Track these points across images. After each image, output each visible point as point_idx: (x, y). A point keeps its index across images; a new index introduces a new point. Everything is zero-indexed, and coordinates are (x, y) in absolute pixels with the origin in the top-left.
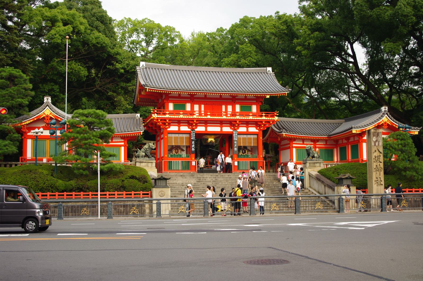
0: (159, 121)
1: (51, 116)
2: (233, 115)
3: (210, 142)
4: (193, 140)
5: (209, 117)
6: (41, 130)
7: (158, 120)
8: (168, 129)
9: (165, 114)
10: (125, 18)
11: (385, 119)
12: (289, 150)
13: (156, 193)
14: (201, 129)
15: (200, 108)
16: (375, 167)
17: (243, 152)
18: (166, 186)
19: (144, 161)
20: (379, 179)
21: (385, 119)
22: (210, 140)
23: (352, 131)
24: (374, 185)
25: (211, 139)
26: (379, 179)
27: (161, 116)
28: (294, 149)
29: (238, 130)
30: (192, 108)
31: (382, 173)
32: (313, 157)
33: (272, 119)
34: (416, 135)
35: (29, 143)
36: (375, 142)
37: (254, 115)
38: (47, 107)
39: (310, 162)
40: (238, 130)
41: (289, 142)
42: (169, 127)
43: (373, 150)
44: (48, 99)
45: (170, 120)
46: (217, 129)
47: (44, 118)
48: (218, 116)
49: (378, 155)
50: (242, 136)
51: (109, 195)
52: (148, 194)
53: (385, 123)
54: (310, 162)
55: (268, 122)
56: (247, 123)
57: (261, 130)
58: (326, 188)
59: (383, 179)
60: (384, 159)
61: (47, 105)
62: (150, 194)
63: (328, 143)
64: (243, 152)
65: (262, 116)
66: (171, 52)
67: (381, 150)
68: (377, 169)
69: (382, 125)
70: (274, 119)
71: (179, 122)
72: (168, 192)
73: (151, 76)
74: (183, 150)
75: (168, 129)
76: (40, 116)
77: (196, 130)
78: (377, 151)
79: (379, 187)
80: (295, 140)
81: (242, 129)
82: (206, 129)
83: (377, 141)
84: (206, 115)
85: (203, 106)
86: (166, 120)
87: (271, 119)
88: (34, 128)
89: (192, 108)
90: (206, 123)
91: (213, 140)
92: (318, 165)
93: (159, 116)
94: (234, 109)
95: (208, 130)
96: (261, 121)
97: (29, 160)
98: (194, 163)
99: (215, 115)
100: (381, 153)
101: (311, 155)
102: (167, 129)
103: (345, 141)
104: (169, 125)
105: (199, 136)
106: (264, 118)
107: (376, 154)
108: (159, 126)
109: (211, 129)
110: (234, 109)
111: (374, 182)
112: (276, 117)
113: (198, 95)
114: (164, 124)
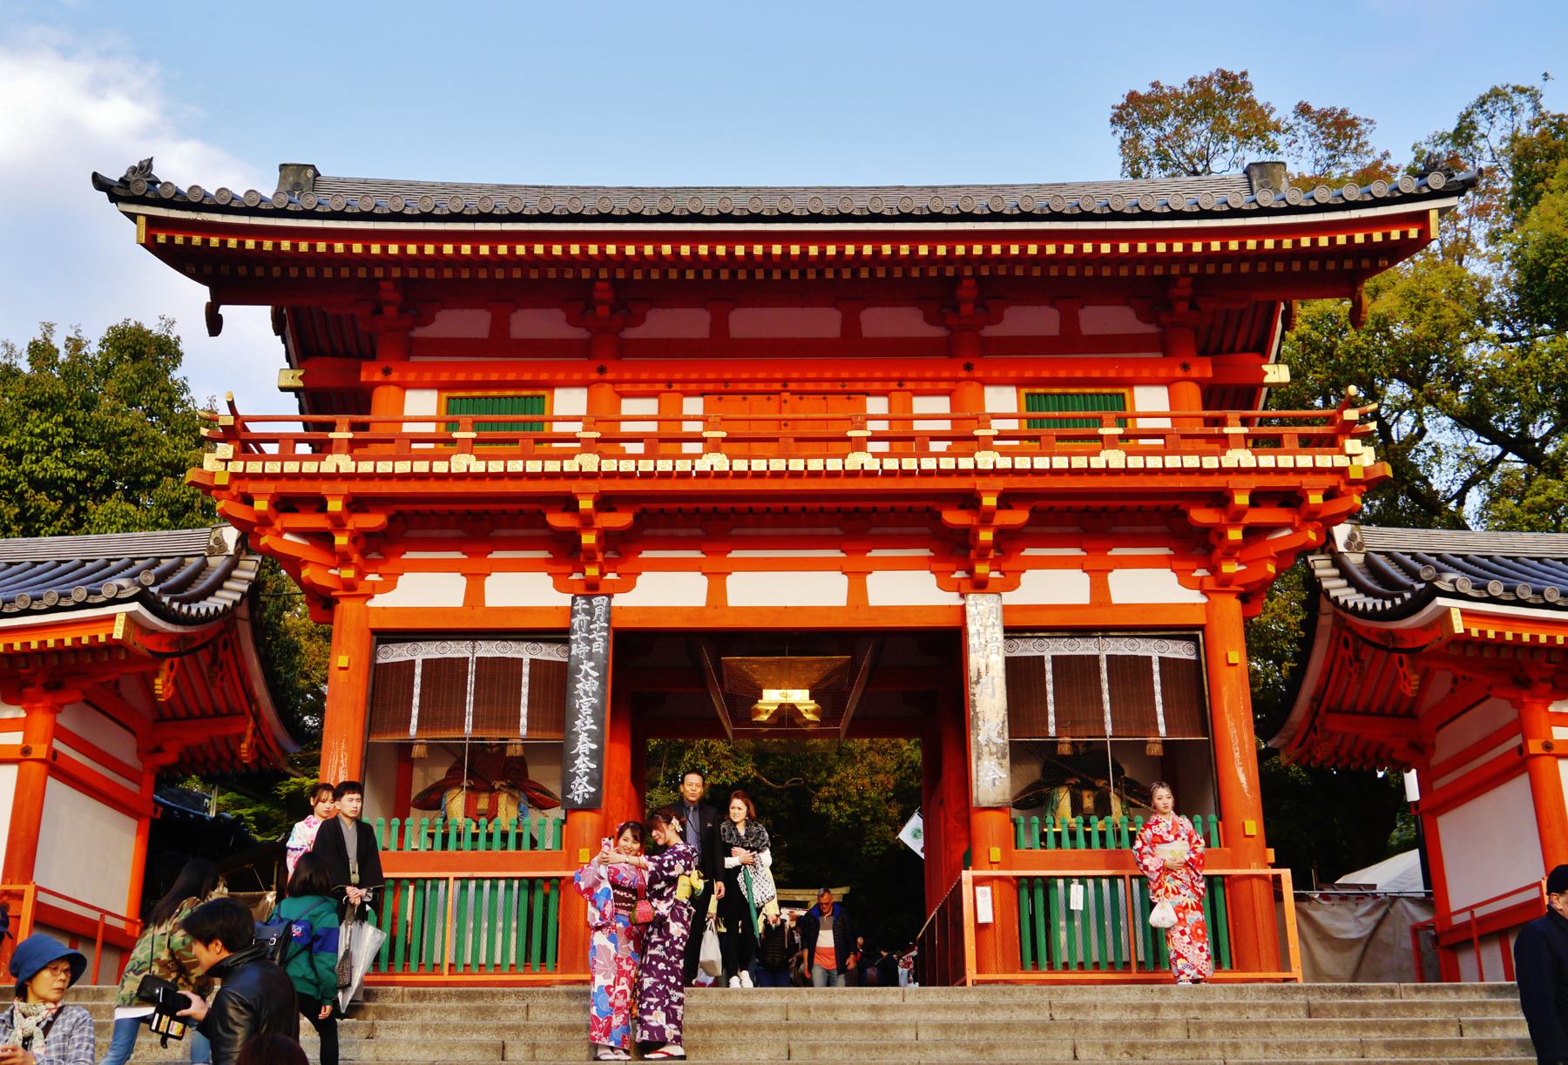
0: (261, 505)
7: (248, 500)
8: (379, 601)
14: (667, 590)
17: (1088, 802)
22: (772, 698)
33: (1324, 461)
55: (1283, 496)
57: (1224, 583)
64: (1088, 802)
65: (1224, 442)
70: (1341, 461)
82: (717, 592)
91: (800, 698)
106: (1239, 457)
112: (1352, 445)
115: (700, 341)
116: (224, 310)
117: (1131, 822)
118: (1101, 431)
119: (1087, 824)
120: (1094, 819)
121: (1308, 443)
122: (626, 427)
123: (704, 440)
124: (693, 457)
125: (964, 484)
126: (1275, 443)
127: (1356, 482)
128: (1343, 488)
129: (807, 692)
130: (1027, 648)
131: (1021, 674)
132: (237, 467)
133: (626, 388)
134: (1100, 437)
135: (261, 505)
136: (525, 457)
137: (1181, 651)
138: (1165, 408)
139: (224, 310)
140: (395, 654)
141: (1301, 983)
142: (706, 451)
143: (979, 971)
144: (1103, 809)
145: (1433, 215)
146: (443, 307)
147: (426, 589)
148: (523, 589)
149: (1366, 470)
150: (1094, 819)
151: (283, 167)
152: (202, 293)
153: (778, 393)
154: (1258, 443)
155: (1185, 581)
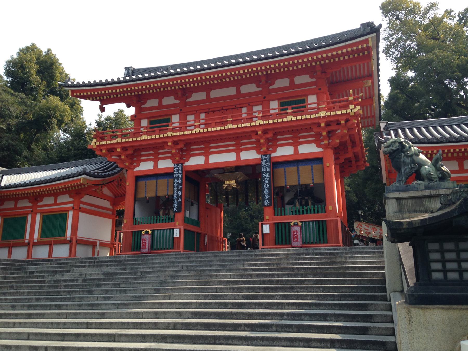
7: (101, 150)
8: (136, 169)
14: (196, 161)
17: (303, 203)
27: (105, 143)
29: (273, 155)
33: (344, 112)
39: (397, 195)
46: (228, 158)
48: (217, 124)
54: (397, 195)
64: (303, 203)
70: (348, 111)
87: (339, 112)
93: (101, 143)
101: (405, 169)
109: (215, 159)
115: (234, 95)
116: (105, 106)
117: (314, 207)
118: (287, 111)
119: (303, 208)
120: (305, 207)
121: (341, 108)
122: (188, 123)
123: (195, 126)
124: (191, 130)
125: (253, 129)
126: (334, 109)
127: (353, 116)
128: (350, 118)
129: (234, 181)
132: (98, 143)
133: (185, 114)
134: (287, 113)
135: (104, 151)
136: (129, 138)
138: (316, 101)
139: (105, 106)
141: (182, 253)
142: (195, 128)
143: (263, 245)
144: (307, 204)
145: (370, 40)
146: (148, 99)
149: (355, 112)
150: (305, 207)
151: (126, 68)
152: (98, 103)
153: (221, 110)
155: (318, 146)
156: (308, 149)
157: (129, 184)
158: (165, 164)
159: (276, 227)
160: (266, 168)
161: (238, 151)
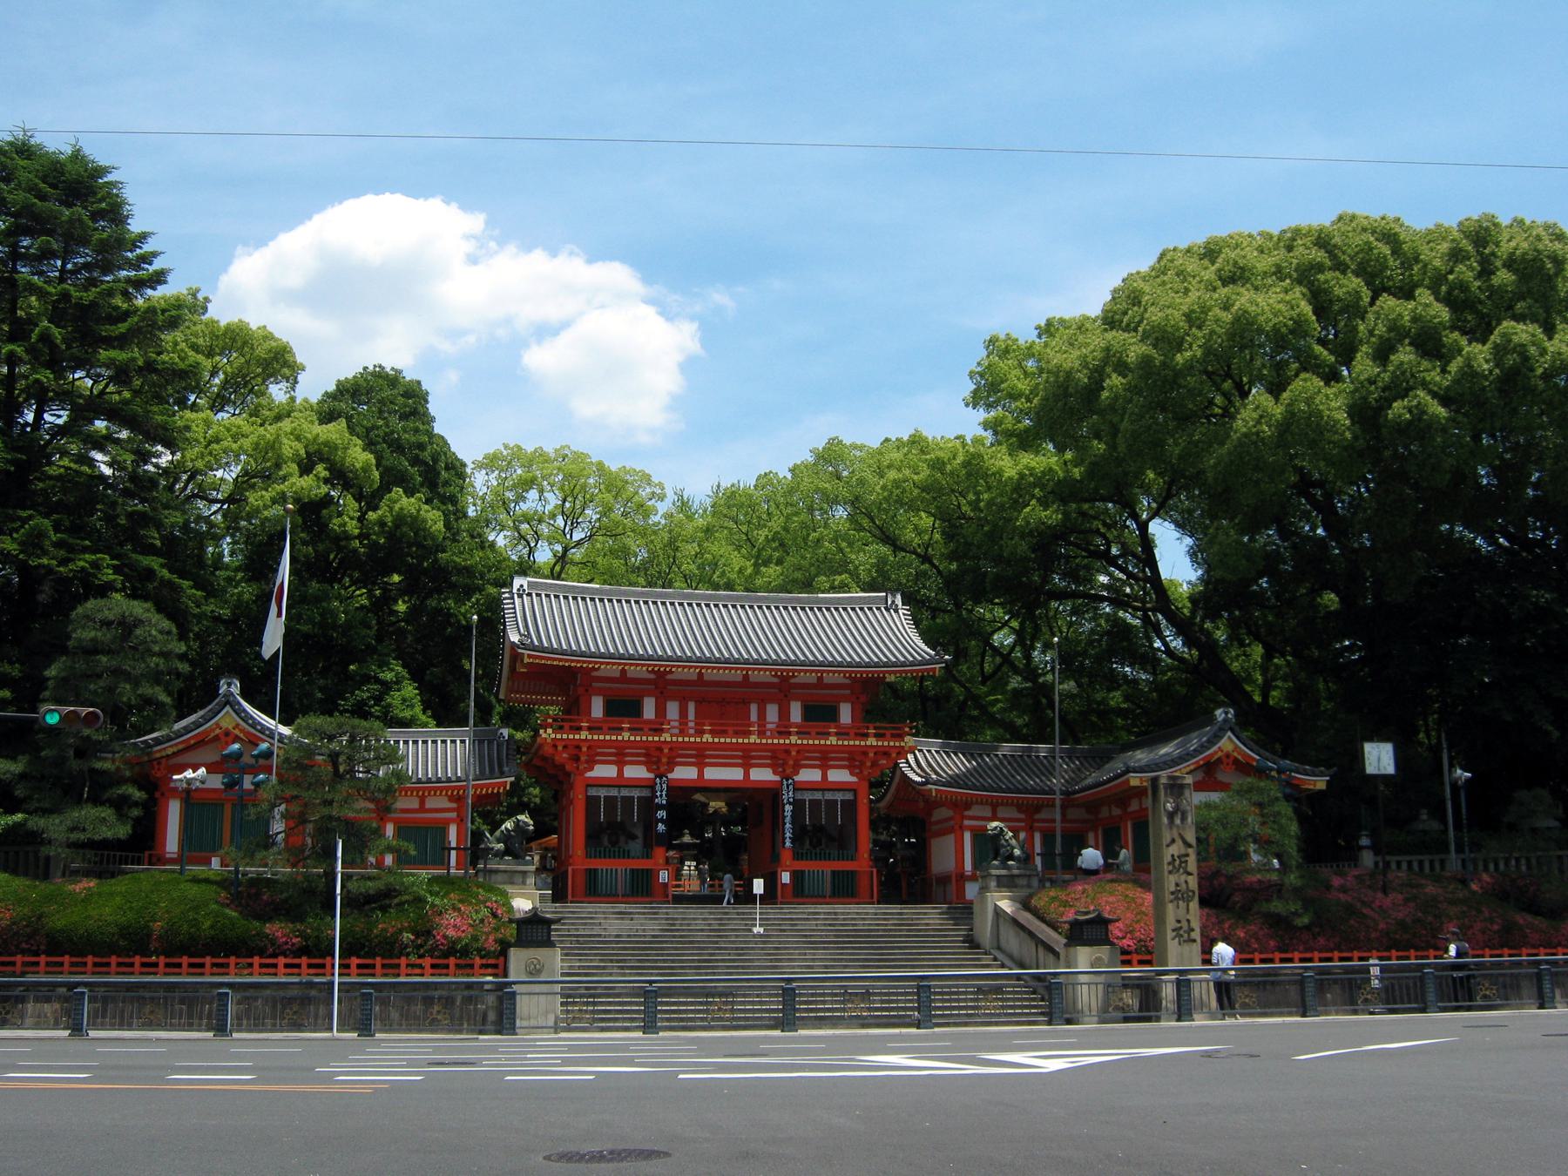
1: (237, 732)
2: (780, 733)
3: (715, 811)
4: (661, 807)
5: (707, 738)
6: (202, 771)
7: (555, 746)
8: (589, 774)
9: (579, 729)
10: (506, 447)
11: (1228, 743)
12: (950, 840)
13: (518, 959)
14: (685, 773)
15: (683, 713)
16: (1172, 888)
18: (548, 943)
19: (502, 867)
20: (1184, 924)
21: (1228, 743)
23: (1128, 781)
24: (1170, 942)
25: (717, 805)
26: (1184, 924)
28: (967, 836)
29: (797, 778)
30: (661, 711)
31: (1194, 905)
32: (1011, 857)
34: (1320, 791)
35: (174, 810)
36: (1171, 816)
37: (841, 734)
38: (228, 708)
40: (797, 778)
41: (950, 813)
42: (592, 769)
43: (1167, 838)
44: (229, 685)
45: (592, 746)
46: (734, 774)
47: (217, 738)
48: (737, 734)
49: (1183, 851)
50: (808, 796)
51: (48, 964)
52: (495, 966)
53: (1228, 755)
55: (885, 753)
56: (825, 759)
58: (1041, 949)
59: (1196, 924)
60: (1199, 867)
61: (227, 703)
62: (501, 967)
63: (1069, 817)
65: (866, 736)
66: (632, 546)
67: (1191, 837)
68: (1180, 895)
69: (1219, 759)
71: (620, 756)
72: (555, 961)
73: (546, 618)
74: (633, 837)
75: (589, 774)
76: (206, 732)
77: (670, 776)
78: (1179, 842)
79: (1186, 947)
80: (968, 805)
81: (810, 775)
82: (701, 773)
83: (1177, 809)
84: (700, 733)
85: (691, 707)
86: (579, 747)
88: (181, 770)
89: (661, 711)
90: (701, 757)
92: (1023, 882)
94: (784, 714)
95: (752, 777)
96: (864, 752)
97: (172, 861)
98: (664, 876)
99: (723, 733)
100: (1190, 846)
102: (582, 774)
103: (1116, 812)
104: (591, 764)
105: (680, 792)
106: (872, 741)
107: (1175, 849)
108: (561, 767)
109: (713, 774)
110: (784, 714)
111: (1170, 934)
113: (679, 674)
114: (577, 759)
130: (799, 796)
131: (798, 805)
137: (849, 796)
140: (593, 792)
147: (605, 771)
148: (636, 772)
154: (878, 736)
156: (839, 775)
157: (579, 797)
158: (636, 772)
159: (796, 876)
160: (787, 795)
161: (747, 767)
